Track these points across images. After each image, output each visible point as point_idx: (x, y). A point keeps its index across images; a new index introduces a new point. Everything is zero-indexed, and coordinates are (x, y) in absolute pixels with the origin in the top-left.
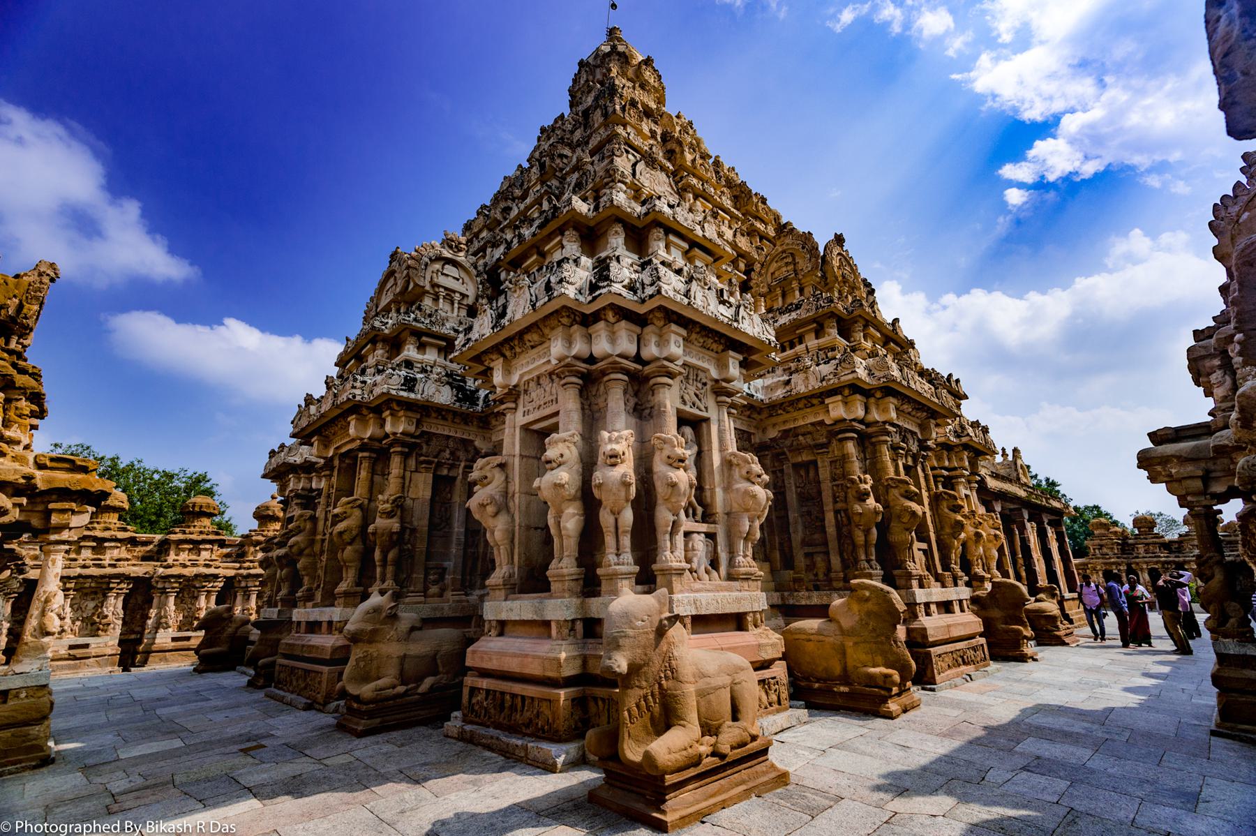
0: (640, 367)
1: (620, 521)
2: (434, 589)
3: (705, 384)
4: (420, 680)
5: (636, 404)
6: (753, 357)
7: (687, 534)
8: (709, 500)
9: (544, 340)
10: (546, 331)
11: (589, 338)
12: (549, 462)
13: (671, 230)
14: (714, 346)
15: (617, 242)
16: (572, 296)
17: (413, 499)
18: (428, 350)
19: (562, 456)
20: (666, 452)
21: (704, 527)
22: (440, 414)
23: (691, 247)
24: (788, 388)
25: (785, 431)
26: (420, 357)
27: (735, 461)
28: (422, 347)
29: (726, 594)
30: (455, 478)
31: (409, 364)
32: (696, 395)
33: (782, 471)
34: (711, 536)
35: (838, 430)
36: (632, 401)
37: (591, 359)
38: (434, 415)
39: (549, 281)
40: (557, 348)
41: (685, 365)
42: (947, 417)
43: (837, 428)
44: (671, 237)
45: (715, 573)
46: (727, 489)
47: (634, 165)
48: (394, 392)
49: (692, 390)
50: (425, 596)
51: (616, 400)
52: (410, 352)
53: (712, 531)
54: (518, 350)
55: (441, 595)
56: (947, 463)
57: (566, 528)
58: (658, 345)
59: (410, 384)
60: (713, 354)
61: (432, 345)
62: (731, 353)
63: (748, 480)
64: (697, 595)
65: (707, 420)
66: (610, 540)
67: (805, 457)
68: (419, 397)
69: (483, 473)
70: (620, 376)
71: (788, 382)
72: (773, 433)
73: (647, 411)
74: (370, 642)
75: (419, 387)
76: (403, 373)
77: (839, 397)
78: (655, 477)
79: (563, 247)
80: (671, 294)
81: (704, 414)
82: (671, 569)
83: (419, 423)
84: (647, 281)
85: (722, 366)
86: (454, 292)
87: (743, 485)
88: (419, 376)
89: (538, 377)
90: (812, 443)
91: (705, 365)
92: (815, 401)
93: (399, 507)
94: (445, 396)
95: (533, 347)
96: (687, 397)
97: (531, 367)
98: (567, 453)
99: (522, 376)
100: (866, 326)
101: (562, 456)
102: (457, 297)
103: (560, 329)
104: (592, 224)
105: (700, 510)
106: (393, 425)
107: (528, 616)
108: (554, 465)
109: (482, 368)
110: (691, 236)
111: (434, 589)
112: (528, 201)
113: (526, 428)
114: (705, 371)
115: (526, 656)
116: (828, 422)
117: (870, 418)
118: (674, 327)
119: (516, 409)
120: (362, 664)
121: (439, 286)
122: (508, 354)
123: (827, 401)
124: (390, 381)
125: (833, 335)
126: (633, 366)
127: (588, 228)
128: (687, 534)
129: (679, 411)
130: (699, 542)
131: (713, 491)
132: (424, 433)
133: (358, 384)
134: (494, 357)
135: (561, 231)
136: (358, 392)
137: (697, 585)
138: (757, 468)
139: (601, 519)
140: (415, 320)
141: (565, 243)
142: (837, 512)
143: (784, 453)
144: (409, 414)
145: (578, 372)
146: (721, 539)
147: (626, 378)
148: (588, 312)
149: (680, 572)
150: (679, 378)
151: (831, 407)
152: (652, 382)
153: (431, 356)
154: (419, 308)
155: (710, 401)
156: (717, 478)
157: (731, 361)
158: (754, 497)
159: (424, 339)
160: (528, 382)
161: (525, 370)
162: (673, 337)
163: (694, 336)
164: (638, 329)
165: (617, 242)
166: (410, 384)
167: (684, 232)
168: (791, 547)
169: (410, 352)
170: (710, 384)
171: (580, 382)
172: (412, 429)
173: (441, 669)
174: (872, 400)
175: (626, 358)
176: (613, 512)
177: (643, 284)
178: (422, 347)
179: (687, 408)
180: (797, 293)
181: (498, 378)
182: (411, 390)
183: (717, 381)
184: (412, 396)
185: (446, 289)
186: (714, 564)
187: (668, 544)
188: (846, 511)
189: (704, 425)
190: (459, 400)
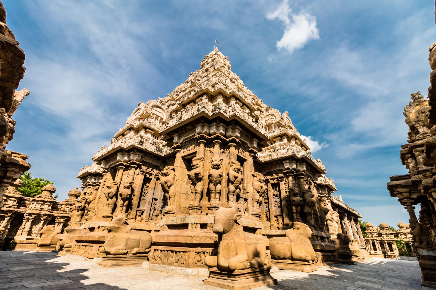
2: (139, 219)
4: (133, 248)
6: (262, 142)
9: (194, 128)
10: (194, 124)
11: (209, 128)
12: (193, 166)
13: (237, 99)
14: (250, 136)
15: (220, 99)
16: (206, 112)
17: (136, 184)
18: (148, 134)
23: (243, 105)
24: (271, 157)
25: (268, 172)
26: (145, 135)
28: (146, 132)
30: (151, 179)
31: (142, 137)
37: (210, 135)
39: (199, 108)
40: (198, 129)
42: (322, 173)
44: (237, 101)
47: (226, 80)
48: (136, 145)
52: (142, 133)
54: (184, 131)
56: (320, 192)
58: (232, 132)
59: (141, 143)
61: (150, 133)
63: (260, 181)
65: (246, 160)
67: (276, 181)
68: (144, 148)
70: (219, 141)
71: (271, 155)
74: (116, 232)
75: (144, 144)
76: (140, 139)
77: (288, 161)
79: (202, 100)
80: (239, 115)
83: (142, 157)
84: (231, 111)
85: (252, 143)
86: (159, 117)
88: (145, 141)
89: (190, 140)
91: (246, 142)
92: (279, 162)
93: (130, 187)
94: (152, 149)
95: (189, 130)
97: (188, 137)
98: (200, 164)
99: (184, 140)
100: (295, 140)
102: (159, 118)
103: (200, 124)
104: (212, 94)
106: (133, 157)
107: (180, 222)
109: (169, 138)
110: (243, 101)
111: (139, 219)
112: (186, 92)
113: (183, 158)
114: (247, 144)
115: (178, 236)
117: (298, 169)
118: (238, 127)
120: (112, 240)
121: (154, 114)
122: (180, 132)
123: (283, 162)
124: (135, 141)
125: (285, 140)
127: (211, 96)
129: (238, 156)
132: (143, 161)
133: (123, 142)
134: (174, 133)
135: (202, 95)
136: (123, 144)
140: (146, 123)
141: (203, 98)
144: (139, 154)
148: (210, 119)
150: (238, 144)
151: (285, 164)
153: (149, 135)
154: (147, 120)
157: (255, 142)
159: (148, 130)
160: (186, 142)
161: (185, 138)
162: (237, 130)
163: (244, 132)
164: (226, 127)
165: (220, 99)
166: (141, 143)
167: (241, 100)
169: (142, 133)
173: (141, 245)
174: (298, 163)
176: (214, 185)
177: (229, 112)
178: (146, 132)
180: (273, 128)
181: (175, 140)
182: (141, 145)
184: (142, 147)
185: (156, 115)
190: (157, 151)
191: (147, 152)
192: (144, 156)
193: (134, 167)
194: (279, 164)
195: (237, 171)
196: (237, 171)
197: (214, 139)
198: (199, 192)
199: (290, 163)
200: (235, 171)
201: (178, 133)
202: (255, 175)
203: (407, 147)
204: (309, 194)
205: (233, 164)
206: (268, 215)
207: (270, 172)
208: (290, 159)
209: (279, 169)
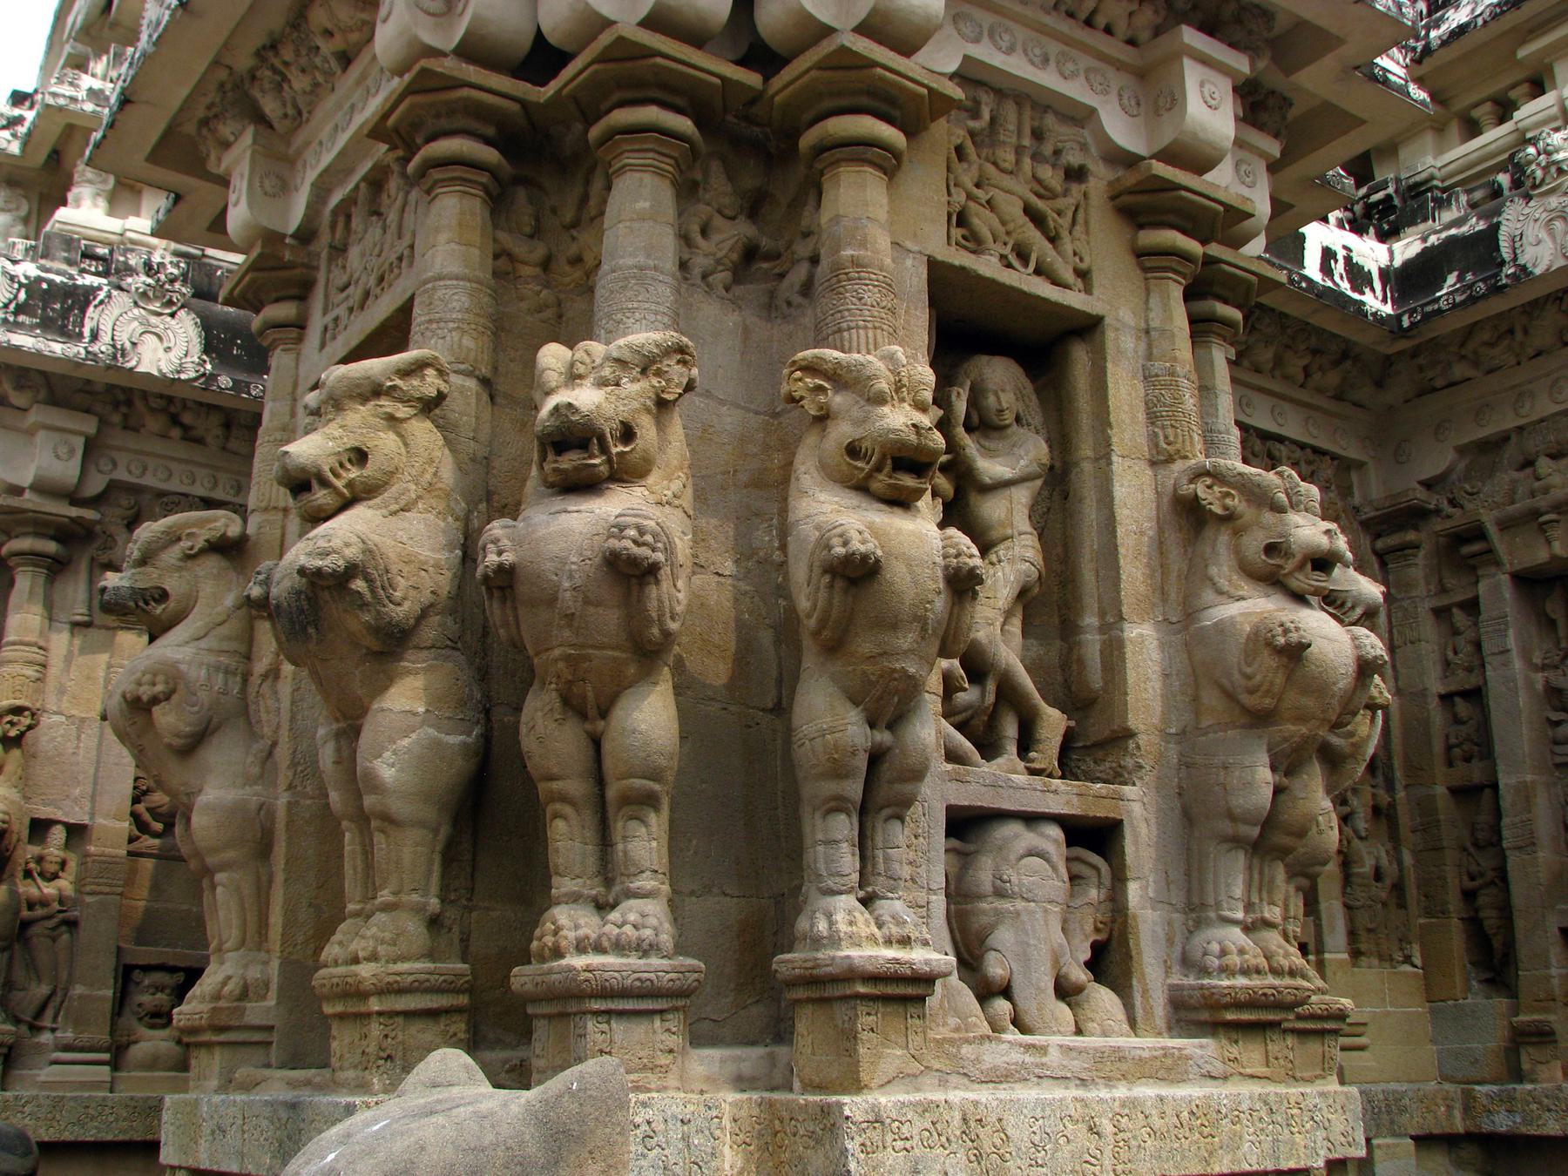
0: (752, 79)
1: (607, 747)
3: (1076, 175)
5: (750, 254)
7: (966, 825)
8: (1095, 678)
19: (360, 456)
20: (842, 431)
21: (1063, 797)
22: (175, 420)
27: (1210, 496)
29: (1147, 1091)
32: (1037, 219)
33: (1472, 606)
34: (1094, 837)
36: (731, 235)
38: (154, 424)
41: (969, 75)
45: (1103, 999)
46: (1183, 621)
49: (1012, 196)
50: (115, 1065)
51: (639, 218)
53: (1101, 811)
55: (184, 1066)
57: (375, 785)
60: (1114, 48)
62: (1190, 36)
63: (1272, 580)
64: (983, 1095)
65: (1088, 327)
66: (568, 839)
69: (148, 578)
72: (1436, 459)
73: (799, 274)
81: (1074, 299)
82: (852, 974)
83: (92, 448)
85: (1154, 88)
87: (1248, 608)
91: (1076, 90)
96: (983, 221)
98: (385, 444)
99: (321, 190)
101: (360, 456)
105: (1053, 722)
108: (321, 497)
111: (152, 1043)
114: (1082, 117)
119: (300, 325)
122: (270, 106)
126: (717, 66)
128: (966, 825)
129: (939, 276)
130: (1032, 867)
131: (1114, 650)
137: (1008, 1049)
138: (1310, 530)
139: (528, 743)
143: (1479, 533)
144: (57, 417)
145: (479, 112)
146: (1143, 841)
147: (684, 124)
149: (904, 992)
152: (808, 140)
155: (1101, 243)
156: (1134, 574)
157: (1192, 75)
158: (1295, 653)
168: (1505, 910)
170: (1101, 178)
171: (490, 155)
172: (67, 470)
175: (696, 36)
176: (573, 705)
179: (987, 266)
183: (1129, 160)
186: (1109, 960)
187: (848, 861)
189: (1080, 356)
191: (145, 395)
192: (118, 438)
193: (34, 557)
195: (881, 482)
197: (588, 105)
198: (399, 807)
200: (862, 488)
201: (260, 119)
205: (838, 400)
206: (1490, 917)
207: (1503, 439)
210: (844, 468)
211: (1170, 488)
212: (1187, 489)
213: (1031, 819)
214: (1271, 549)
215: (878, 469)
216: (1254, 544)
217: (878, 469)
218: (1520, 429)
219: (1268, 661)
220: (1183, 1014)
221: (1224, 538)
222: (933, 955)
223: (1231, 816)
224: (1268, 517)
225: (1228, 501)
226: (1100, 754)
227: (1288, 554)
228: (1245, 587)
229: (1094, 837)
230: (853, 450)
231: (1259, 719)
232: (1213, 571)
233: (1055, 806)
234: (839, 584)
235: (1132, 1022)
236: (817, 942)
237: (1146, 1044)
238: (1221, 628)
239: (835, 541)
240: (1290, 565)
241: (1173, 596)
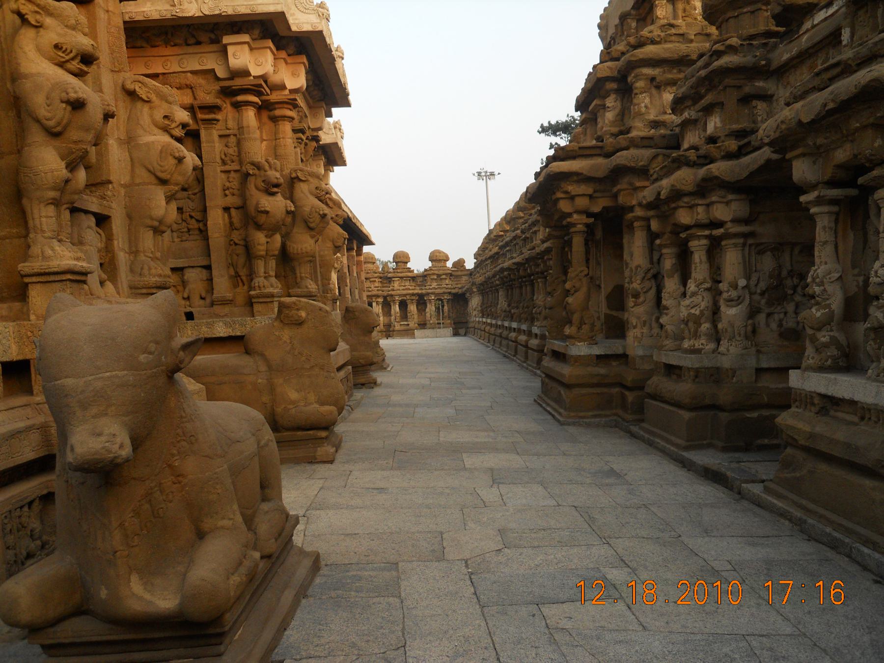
34: (102, 220)
35: (236, 89)
43: (238, 82)
46: (129, 141)
63: (166, 130)
77: (246, 38)
78: (27, 85)
90: (196, 103)
92: (204, 37)
116: (221, 73)
123: (226, 40)
142: (226, 209)
146: (118, 224)
151: (231, 50)
158: (180, 160)
174: (283, 54)
188: (242, 208)
194: (198, 43)
196: (75, 65)
199: (251, 49)
200: (61, 65)
202: (142, 92)
203: (617, 59)
204: (313, 187)
208: (257, 32)
209: (198, 67)
210: (52, 54)
211: (120, 81)
212: (130, 86)
213: (86, 212)
214: (166, 117)
215: (73, 59)
216: (159, 116)
217: (73, 59)
218: (164, 74)
219: (173, 162)
220: (133, 291)
221: (146, 109)
222: (92, 265)
223: (152, 219)
224: (165, 105)
225: (149, 95)
226: (94, 189)
227: (173, 121)
228: (156, 130)
229: (102, 220)
230: (57, 47)
231: (163, 182)
232: (142, 122)
233: (94, 208)
234: (69, 108)
235: (118, 293)
236: (45, 258)
237: (123, 300)
238: (147, 145)
239: (70, 90)
240: (173, 125)
241: (122, 128)
